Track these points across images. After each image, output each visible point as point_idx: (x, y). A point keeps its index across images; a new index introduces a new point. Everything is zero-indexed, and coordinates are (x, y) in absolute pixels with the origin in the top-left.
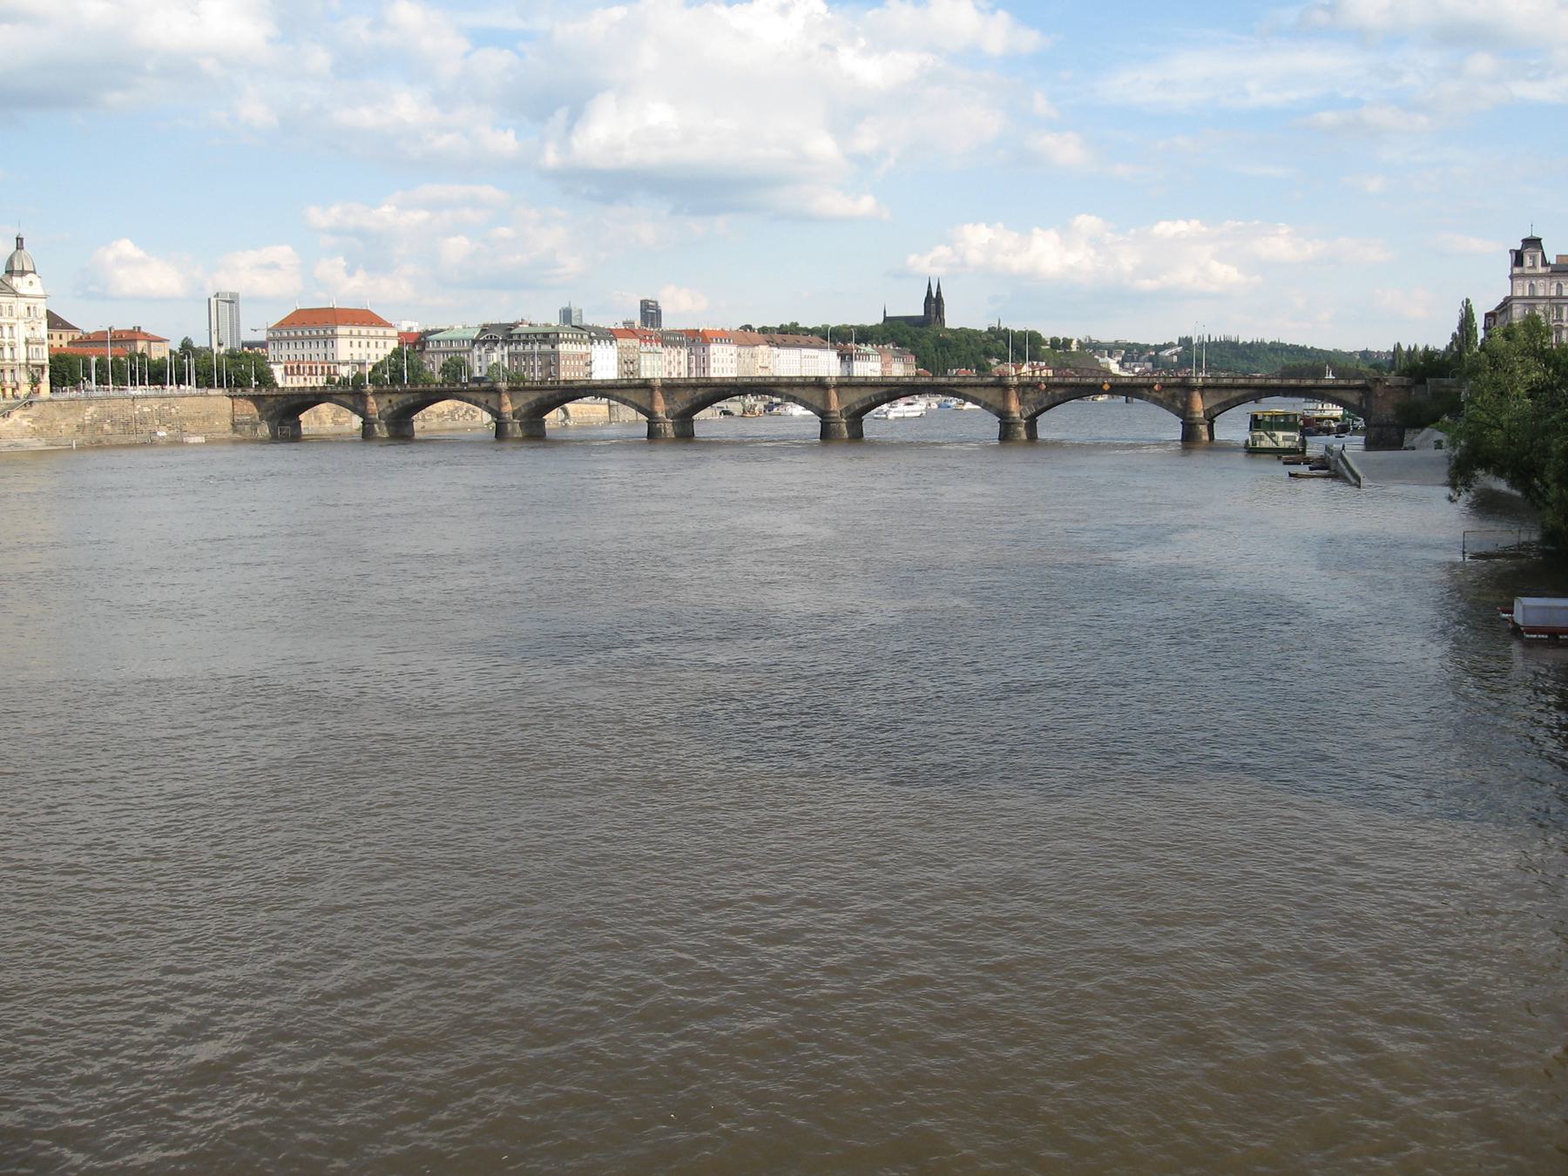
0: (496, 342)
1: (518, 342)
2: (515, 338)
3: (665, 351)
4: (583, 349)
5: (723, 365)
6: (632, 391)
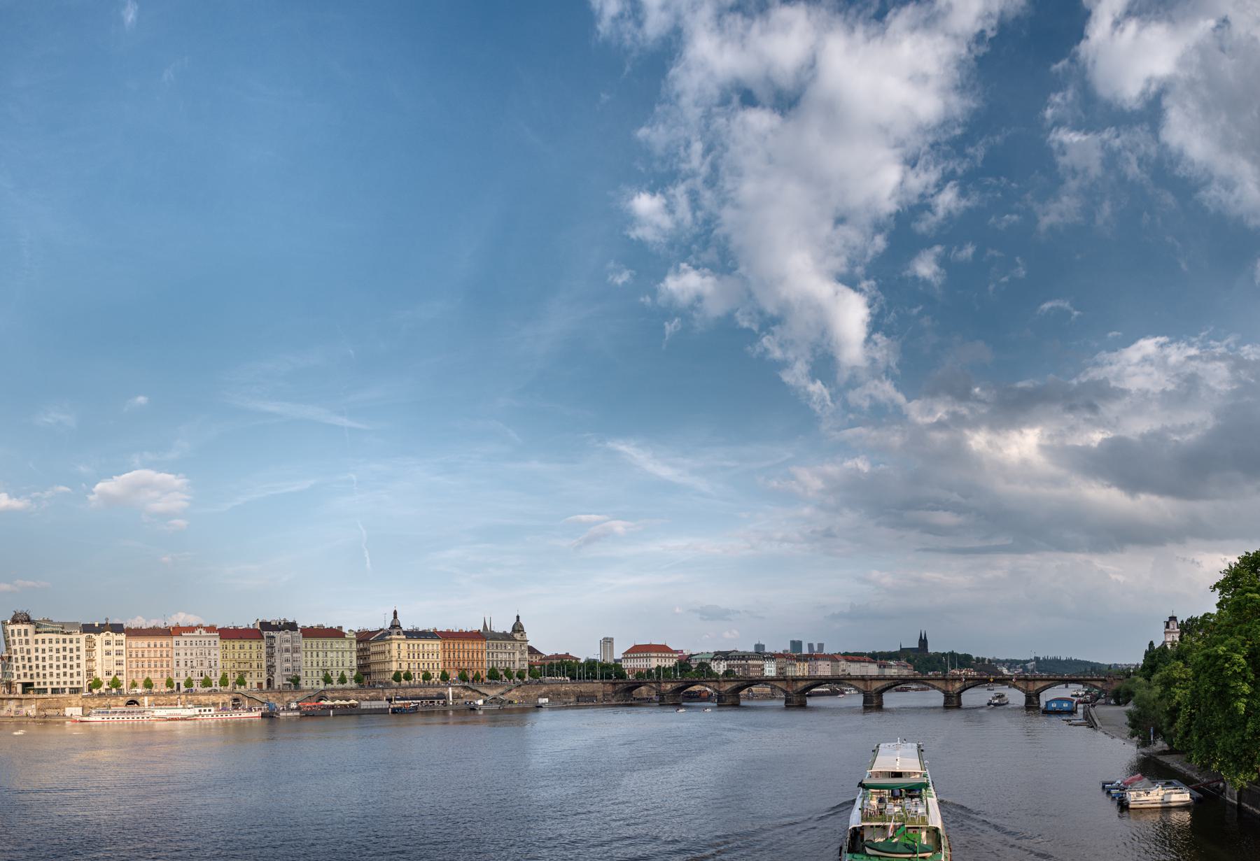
0: (721, 660)
1: (731, 660)
2: (730, 657)
4: (760, 662)
6: (778, 682)
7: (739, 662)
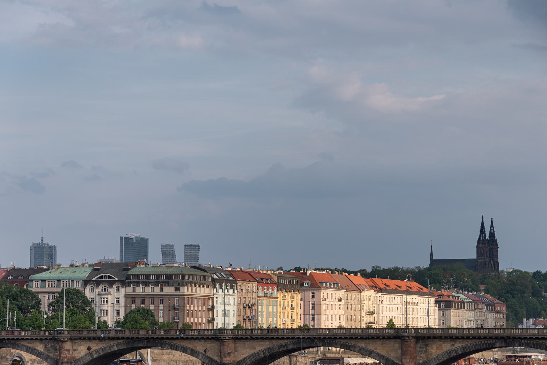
0: (111, 283)
1: (137, 284)
2: (134, 279)
3: (280, 295)
4: (205, 292)
5: (332, 312)
6: (378, 342)
7: (157, 290)
